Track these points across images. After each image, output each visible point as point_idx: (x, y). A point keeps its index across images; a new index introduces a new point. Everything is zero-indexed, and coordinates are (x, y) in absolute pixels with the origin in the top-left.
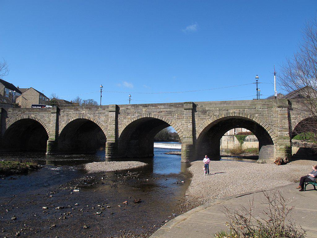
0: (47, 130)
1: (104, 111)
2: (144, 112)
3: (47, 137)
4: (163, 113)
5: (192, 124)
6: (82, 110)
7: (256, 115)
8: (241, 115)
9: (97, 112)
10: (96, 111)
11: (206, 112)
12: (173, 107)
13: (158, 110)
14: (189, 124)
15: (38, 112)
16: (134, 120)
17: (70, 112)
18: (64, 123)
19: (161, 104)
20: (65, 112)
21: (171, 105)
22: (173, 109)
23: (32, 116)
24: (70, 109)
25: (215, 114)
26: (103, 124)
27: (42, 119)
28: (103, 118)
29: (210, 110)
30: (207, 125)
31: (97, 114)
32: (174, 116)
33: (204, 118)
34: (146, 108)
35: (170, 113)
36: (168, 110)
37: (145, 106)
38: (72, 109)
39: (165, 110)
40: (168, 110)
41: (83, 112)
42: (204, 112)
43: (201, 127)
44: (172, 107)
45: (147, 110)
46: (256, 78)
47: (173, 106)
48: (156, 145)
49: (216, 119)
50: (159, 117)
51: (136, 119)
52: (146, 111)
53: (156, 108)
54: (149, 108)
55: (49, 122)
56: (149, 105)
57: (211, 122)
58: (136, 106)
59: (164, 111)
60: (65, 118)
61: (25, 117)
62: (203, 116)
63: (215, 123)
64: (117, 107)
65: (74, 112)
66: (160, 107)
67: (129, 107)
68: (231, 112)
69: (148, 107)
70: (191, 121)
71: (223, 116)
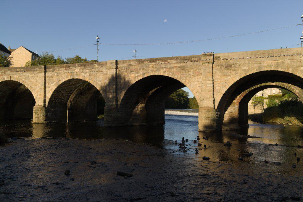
1: (101, 69)
2: (150, 69)
3: (34, 103)
4: (175, 69)
6: (75, 68)
8: (280, 69)
9: (93, 70)
11: (231, 67)
16: (139, 79)
17: (61, 71)
18: (54, 84)
19: (172, 58)
21: (185, 59)
22: (188, 64)
24: (61, 67)
25: (243, 68)
30: (233, 83)
32: (190, 73)
34: (154, 63)
35: (184, 68)
36: (181, 65)
38: (63, 67)
39: (176, 65)
41: (76, 71)
42: (228, 66)
43: (225, 86)
47: (187, 60)
49: (243, 75)
50: (171, 74)
51: (142, 78)
52: (153, 67)
55: (35, 84)
56: (157, 59)
57: (238, 79)
60: (55, 78)
61: (6, 78)
62: (226, 71)
64: (117, 61)
65: (65, 71)
66: (169, 61)
67: (132, 63)
68: (266, 65)
69: (156, 62)
71: (255, 71)
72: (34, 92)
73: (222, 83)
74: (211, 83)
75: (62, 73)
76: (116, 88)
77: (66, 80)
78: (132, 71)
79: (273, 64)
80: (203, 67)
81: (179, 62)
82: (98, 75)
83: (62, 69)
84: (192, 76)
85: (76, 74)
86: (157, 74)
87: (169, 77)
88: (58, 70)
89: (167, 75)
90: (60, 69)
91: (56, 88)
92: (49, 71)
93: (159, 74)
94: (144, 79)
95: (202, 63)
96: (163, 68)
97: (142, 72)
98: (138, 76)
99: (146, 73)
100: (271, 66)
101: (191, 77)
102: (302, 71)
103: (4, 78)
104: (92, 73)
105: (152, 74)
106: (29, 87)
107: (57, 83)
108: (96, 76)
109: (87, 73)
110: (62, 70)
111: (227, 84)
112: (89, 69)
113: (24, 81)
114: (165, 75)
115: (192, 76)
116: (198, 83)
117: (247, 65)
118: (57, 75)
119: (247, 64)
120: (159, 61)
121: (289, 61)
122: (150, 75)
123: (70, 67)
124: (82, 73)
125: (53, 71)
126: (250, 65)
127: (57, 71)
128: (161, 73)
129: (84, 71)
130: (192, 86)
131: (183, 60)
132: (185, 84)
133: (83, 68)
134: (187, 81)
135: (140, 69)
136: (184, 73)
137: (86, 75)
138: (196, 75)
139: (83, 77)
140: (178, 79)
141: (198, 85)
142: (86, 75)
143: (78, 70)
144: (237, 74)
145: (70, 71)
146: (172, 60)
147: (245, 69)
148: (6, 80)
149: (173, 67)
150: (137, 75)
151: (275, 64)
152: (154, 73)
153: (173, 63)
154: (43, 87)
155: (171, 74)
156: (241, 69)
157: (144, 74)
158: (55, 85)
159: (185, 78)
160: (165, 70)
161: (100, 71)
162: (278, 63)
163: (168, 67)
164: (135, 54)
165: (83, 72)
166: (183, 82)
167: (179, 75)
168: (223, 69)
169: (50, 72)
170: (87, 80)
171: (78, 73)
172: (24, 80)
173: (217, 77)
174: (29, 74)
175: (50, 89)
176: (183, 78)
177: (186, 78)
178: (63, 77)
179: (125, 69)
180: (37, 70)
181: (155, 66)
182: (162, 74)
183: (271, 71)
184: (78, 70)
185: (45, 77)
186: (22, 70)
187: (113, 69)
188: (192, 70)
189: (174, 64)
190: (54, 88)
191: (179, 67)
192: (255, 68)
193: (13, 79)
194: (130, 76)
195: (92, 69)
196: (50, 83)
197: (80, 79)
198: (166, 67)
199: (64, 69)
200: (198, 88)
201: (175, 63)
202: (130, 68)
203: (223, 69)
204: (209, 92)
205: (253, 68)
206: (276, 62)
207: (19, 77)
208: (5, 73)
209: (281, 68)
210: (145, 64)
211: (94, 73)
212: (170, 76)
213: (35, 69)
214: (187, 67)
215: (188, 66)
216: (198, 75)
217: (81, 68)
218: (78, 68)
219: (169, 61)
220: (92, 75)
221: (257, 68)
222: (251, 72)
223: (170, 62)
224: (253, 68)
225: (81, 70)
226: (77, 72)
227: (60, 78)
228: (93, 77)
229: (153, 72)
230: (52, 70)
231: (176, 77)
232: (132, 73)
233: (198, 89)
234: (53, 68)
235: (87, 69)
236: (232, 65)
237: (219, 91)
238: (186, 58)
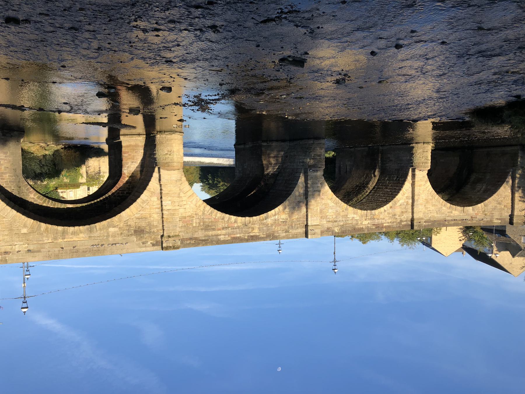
1: (330, 225)
2: (257, 226)
3: (430, 174)
4: (220, 226)
6: (369, 225)
7: (24, 231)
8: (60, 228)
9: (342, 223)
11: (135, 231)
13: (230, 230)
15: (448, 218)
16: (273, 212)
17: (390, 221)
18: (401, 202)
19: (225, 242)
20: (399, 221)
21: (205, 242)
22: (200, 234)
24: (389, 227)
26: (329, 201)
32: (198, 221)
34: (252, 234)
35: (207, 228)
36: (210, 233)
38: (386, 227)
39: (219, 232)
40: (210, 233)
42: (139, 232)
43: (143, 202)
44: (203, 238)
46: (27, 308)
47: (203, 240)
48: (228, 161)
49: (116, 219)
50: (226, 219)
51: (269, 212)
52: (253, 229)
53: (233, 236)
54: (247, 235)
55: (427, 201)
56: (247, 240)
57: (123, 213)
58: (271, 236)
59: (219, 230)
60: (398, 211)
62: (143, 224)
64: (307, 236)
65: (383, 221)
66: (228, 238)
67: (284, 234)
68: (81, 235)
69: (248, 236)
71: (98, 225)
73: (148, 207)
74: (166, 206)
75: (388, 218)
76: (308, 197)
77: (382, 209)
78: (283, 222)
79: (71, 236)
80: (178, 229)
81: (214, 237)
82: (334, 216)
83: (387, 224)
84: (194, 217)
85: (367, 218)
86: (247, 218)
87: (229, 214)
88: (393, 223)
89: (232, 216)
90: (390, 224)
91: (397, 197)
92: (406, 221)
93: (244, 218)
94: (267, 211)
95: (179, 236)
96: (238, 227)
97: (269, 221)
98: (275, 215)
99: (263, 220)
100: (74, 233)
101: (196, 214)
102: (25, 226)
103: (473, 210)
104: (344, 219)
105: (254, 218)
106: (436, 198)
107: (396, 203)
108: (338, 214)
109: (350, 219)
110: (388, 223)
111: (140, 206)
112: (348, 225)
113: (444, 205)
114: (235, 217)
115: (194, 217)
116: (185, 206)
117: (110, 234)
118: (395, 215)
119: (110, 236)
120: (245, 238)
121: (45, 242)
122: (258, 217)
123: (376, 228)
124: (358, 218)
125: (401, 221)
126: (106, 234)
127: (396, 222)
128: (240, 220)
129: (354, 222)
130: (194, 202)
131: (208, 240)
132: (205, 204)
133: (357, 227)
134: (202, 208)
135: (272, 225)
137: (352, 216)
138: (188, 219)
139: (357, 214)
140: (216, 211)
141: (185, 203)
142: (352, 216)
143: (363, 224)
144: (125, 220)
145: (376, 222)
146: (224, 239)
147: (114, 228)
148: (471, 208)
149: (223, 229)
150: (277, 216)
151: (67, 237)
152: (252, 220)
153: (223, 235)
154: (416, 198)
155: (226, 219)
156: (119, 228)
157: (266, 218)
158: (399, 201)
159: (206, 212)
160: (236, 225)
161: (332, 221)
162: (63, 239)
163: (230, 229)
164: (280, 247)
165: (357, 220)
166: (208, 207)
167: (214, 217)
168: (148, 228)
169: (405, 219)
170: (350, 209)
171: (363, 218)
172: (444, 208)
174: (437, 216)
175: (406, 195)
176: (208, 213)
177: (203, 214)
178: (386, 213)
179: (293, 225)
180: (425, 222)
181: (250, 230)
182: (240, 218)
183: (74, 225)
184: (363, 224)
185: (413, 213)
186: (447, 223)
187: (312, 226)
188: (194, 225)
189: (222, 234)
191: (214, 229)
192: (98, 229)
193: (459, 208)
194: (287, 216)
195: (343, 226)
196: (405, 204)
197: (361, 209)
198: (234, 229)
199: (385, 225)
200: (184, 199)
201: (221, 235)
202: (286, 227)
203: (148, 228)
204: (168, 192)
205: (100, 229)
206: (65, 240)
207: (452, 212)
208: (472, 217)
209: (57, 230)
210: (265, 233)
211: (341, 219)
212: (227, 216)
213: (427, 224)
214: (202, 229)
215: (200, 230)
216: (185, 218)
217: (359, 227)
218: (364, 227)
219: (229, 238)
220: (343, 217)
221: (95, 229)
222: (104, 223)
223: (227, 236)
224: (100, 229)
225: (359, 222)
226: (366, 220)
227: (391, 211)
228: (342, 214)
229: (253, 222)
230: (403, 223)
232: (283, 219)
233: (185, 196)
234: (401, 226)
235: (351, 225)
236: (133, 233)
237: (153, 193)
238: (204, 243)
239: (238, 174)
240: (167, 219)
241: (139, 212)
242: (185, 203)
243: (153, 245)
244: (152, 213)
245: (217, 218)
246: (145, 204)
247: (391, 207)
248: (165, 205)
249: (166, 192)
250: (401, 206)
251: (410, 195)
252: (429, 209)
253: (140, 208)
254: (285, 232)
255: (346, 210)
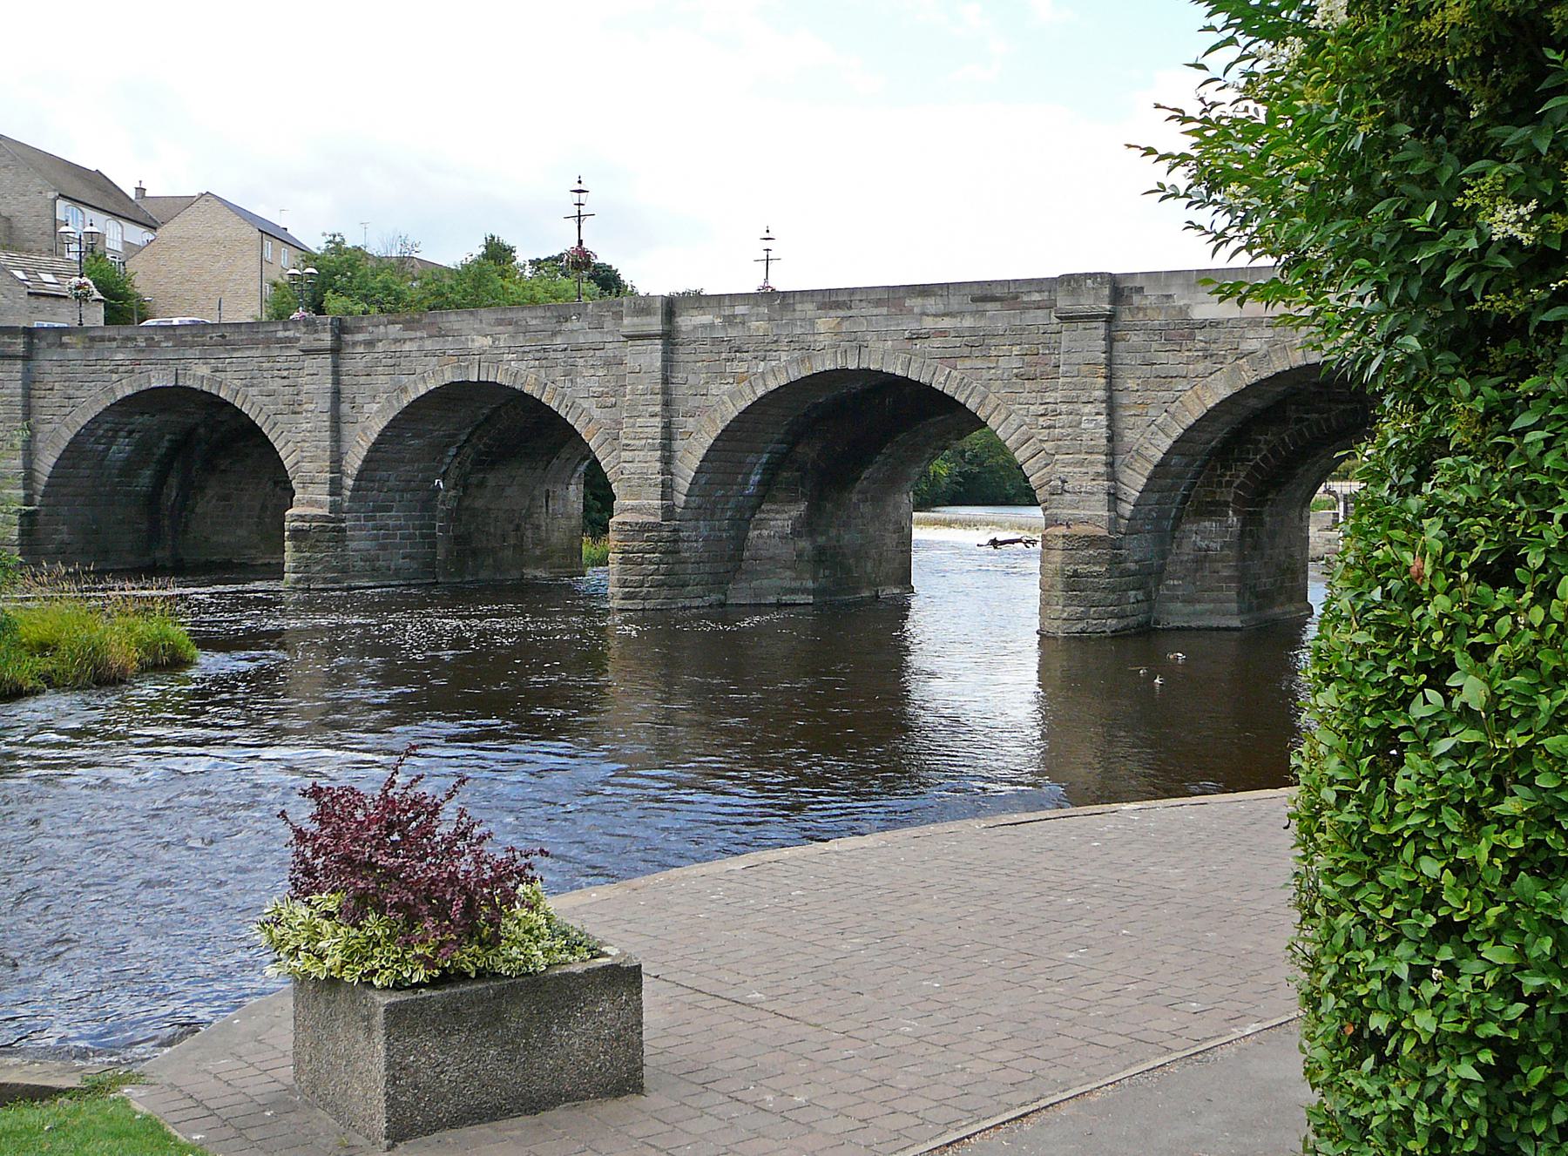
0: (282, 454)
5: (1102, 410)
9: (559, 340)
10: (554, 334)
12: (998, 305)
14: (1088, 409)
16: (773, 385)
17: (407, 347)
18: (375, 407)
19: (924, 290)
21: (984, 294)
22: (997, 318)
23: (198, 374)
25: (1246, 346)
26: (596, 413)
27: (253, 391)
28: (591, 379)
29: (1215, 324)
31: (559, 355)
32: (1003, 362)
33: (1182, 369)
34: (841, 313)
35: (978, 343)
36: (968, 322)
37: (831, 300)
40: (968, 322)
44: (989, 306)
45: (846, 326)
47: (994, 299)
49: (1248, 377)
51: (783, 380)
55: (295, 408)
62: (1170, 360)
63: (1253, 402)
65: (429, 345)
67: (740, 310)
70: (1100, 394)
72: (286, 444)
74: (1097, 414)
81: (955, 307)
88: (396, 341)
92: (355, 344)
105: (829, 366)
111: (1173, 417)
132: (981, 414)
134: (992, 400)
136: (979, 363)
145: (449, 344)
152: (839, 359)
166: (971, 405)
167: (954, 373)
173: (1132, 384)
185: (336, 372)
190: (378, 425)
212: (913, 376)
231: (940, 381)
233: (1041, 441)
239: (907, 499)
240: (1095, 375)
241: (1177, 398)
242: (1041, 419)
243: (1140, 290)
244: (1139, 393)
245: (948, 370)
246: (1160, 420)
247: (404, 390)
248: (1100, 417)
249: (1095, 457)
250: (373, 393)
251: (346, 429)
252: (286, 382)
253: (1172, 410)
254: (735, 316)
255: (546, 384)
